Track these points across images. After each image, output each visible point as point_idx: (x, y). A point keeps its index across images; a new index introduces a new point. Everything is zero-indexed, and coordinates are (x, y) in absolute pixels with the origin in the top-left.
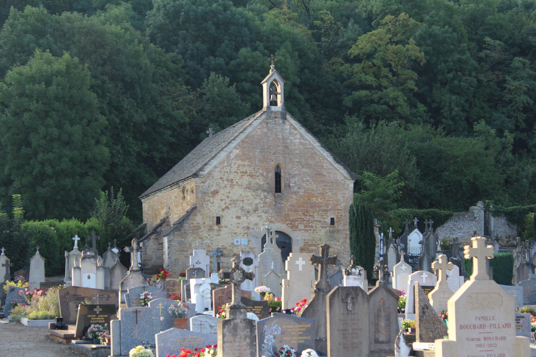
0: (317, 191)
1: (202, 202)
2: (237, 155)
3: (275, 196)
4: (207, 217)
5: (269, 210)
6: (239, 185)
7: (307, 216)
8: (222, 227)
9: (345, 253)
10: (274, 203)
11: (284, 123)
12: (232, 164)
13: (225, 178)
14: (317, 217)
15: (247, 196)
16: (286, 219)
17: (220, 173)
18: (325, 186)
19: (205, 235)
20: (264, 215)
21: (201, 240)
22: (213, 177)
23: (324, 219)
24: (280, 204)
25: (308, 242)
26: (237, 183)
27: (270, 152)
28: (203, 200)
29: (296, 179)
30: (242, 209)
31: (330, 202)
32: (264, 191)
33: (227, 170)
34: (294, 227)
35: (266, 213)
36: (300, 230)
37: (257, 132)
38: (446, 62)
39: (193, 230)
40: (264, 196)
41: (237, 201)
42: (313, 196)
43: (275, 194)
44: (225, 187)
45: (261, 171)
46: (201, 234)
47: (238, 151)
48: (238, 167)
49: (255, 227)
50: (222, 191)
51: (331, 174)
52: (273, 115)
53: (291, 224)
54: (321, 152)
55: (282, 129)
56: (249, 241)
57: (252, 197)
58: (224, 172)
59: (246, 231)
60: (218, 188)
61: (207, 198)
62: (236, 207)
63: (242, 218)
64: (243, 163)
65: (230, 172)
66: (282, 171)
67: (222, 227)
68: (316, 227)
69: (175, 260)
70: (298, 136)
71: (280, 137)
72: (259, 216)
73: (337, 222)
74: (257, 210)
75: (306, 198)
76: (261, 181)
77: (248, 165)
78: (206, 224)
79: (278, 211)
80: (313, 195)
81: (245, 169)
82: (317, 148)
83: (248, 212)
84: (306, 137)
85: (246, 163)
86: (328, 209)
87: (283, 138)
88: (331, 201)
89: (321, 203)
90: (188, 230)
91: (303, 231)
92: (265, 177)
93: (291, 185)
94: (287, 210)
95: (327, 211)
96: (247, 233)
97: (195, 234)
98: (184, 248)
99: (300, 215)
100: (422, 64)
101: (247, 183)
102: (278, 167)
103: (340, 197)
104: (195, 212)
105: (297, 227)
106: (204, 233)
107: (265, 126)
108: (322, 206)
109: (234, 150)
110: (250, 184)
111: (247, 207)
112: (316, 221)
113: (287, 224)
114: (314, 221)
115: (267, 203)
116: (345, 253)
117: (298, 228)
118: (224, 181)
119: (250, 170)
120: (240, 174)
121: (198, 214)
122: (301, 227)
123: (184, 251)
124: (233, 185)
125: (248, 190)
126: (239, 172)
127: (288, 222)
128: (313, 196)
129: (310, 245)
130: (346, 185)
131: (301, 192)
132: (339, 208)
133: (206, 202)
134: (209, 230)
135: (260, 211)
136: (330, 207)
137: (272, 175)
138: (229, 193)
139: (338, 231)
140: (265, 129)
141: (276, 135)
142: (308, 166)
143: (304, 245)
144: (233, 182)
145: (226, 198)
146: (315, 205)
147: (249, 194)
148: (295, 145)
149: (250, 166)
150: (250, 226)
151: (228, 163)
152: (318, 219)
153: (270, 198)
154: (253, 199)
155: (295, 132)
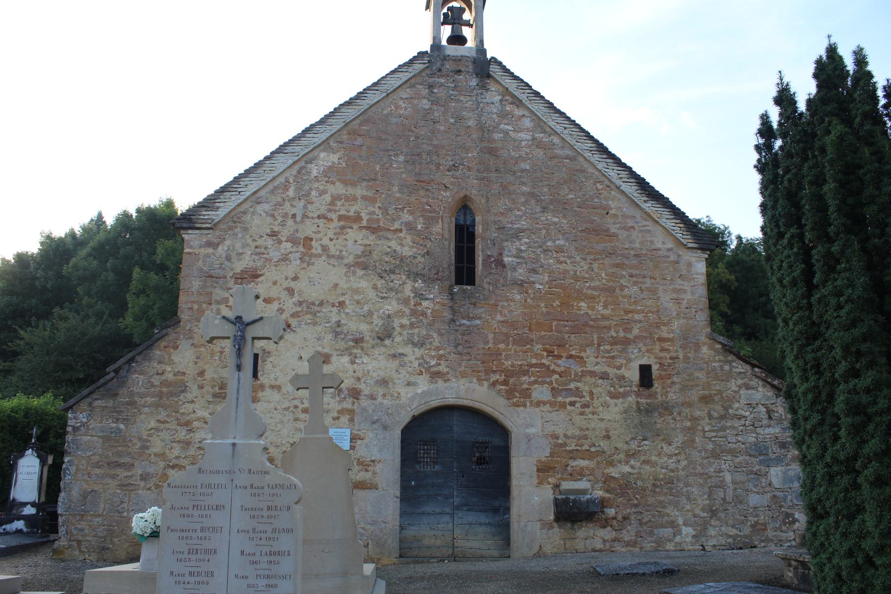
0: (592, 279)
1: (199, 303)
2: (330, 167)
3: (451, 294)
4: (212, 355)
5: (429, 336)
6: (329, 256)
7: (559, 357)
8: (262, 387)
9: (691, 480)
10: (447, 314)
11: (484, 87)
12: (314, 193)
13: (285, 234)
14: (593, 362)
15: (357, 291)
16: (488, 367)
17: (269, 220)
18: (617, 266)
19: (200, 413)
20: (413, 354)
21: (182, 434)
22: (245, 229)
23: (619, 368)
24: (470, 319)
25: (565, 445)
26: (325, 248)
27: (438, 165)
28: (202, 299)
29: (523, 243)
30: (337, 331)
31: (637, 317)
32: (415, 275)
33: (294, 211)
34: (518, 395)
35: (421, 344)
36: (539, 404)
37: (397, 107)
38: (756, 287)
39: (160, 395)
40: (414, 290)
41: (321, 304)
42: (581, 296)
43: (451, 287)
44: (285, 259)
45: (407, 217)
46: (186, 408)
47: (334, 158)
48: (332, 203)
49: (381, 391)
50: (270, 274)
51: (635, 234)
52: (448, 66)
53: (505, 383)
54: (600, 166)
55: (478, 104)
56: (353, 439)
57: (371, 294)
58: (285, 215)
59: (347, 405)
60: (259, 264)
61: (219, 293)
62: (315, 324)
63: (334, 359)
64: (351, 191)
65: (305, 216)
66: (478, 219)
67: (262, 387)
68: (591, 393)
69: (84, 496)
70: (527, 123)
71: (471, 123)
72: (394, 356)
73: (661, 377)
74: (389, 336)
75: (557, 303)
76: (405, 247)
77: (364, 198)
78: (208, 375)
79: (463, 342)
80: (579, 292)
81: (353, 209)
82: (587, 154)
83: (358, 341)
84: (552, 124)
85: (359, 191)
86: (630, 336)
87: (481, 127)
88: (638, 312)
89: (604, 318)
90: (142, 396)
91: (547, 407)
92: (419, 233)
93: (506, 260)
94: (491, 336)
95: (626, 342)
96: (351, 412)
97: (166, 407)
98: (119, 454)
99: (536, 356)
100: (733, 288)
101: (359, 250)
102: (465, 207)
103: (666, 300)
104: (172, 336)
105: (526, 394)
106: (197, 406)
107: (425, 92)
108: (609, 328)
109: (322, 155)
110: (368, 252)
111: (354, 326)
112: (592, 374)
113: (494, 384)
114: (584, 374)
115: (424, 314)
116: (691, 480)
117: (529, 396)
118: (280, 242)
119: (373, 213)
120: (336, 224)
121: (184, 345)
122: (541, 393)
123: (119, 465)
124: (311, 256)
125: (360, 272)
126: (334, 216)
127: (494, 377)
128: (581, 296)
129: (573, 455)
130: (682, 266)
131: (540, 283)
132: (665, 335)
133: (214, 307)
134: (215, 396)
135: (398, 339)
136: (636, 332)
137: (443, 230)
138: (295, 278)
139: (667, 408)
140: (425, 101)
141: (459, 119)
142: (561, 206)
143: (552, 454)
144: (311, 248)
145: (284, 295)
146: (586, 324)
147: (363, 283)
148: (518, 148)
149: (372, 200)
150: (362, 386)
151: (298, 189)
152: (597, 369)
153: (434, 300)
154: (373, 301)
155: (518, 112)
